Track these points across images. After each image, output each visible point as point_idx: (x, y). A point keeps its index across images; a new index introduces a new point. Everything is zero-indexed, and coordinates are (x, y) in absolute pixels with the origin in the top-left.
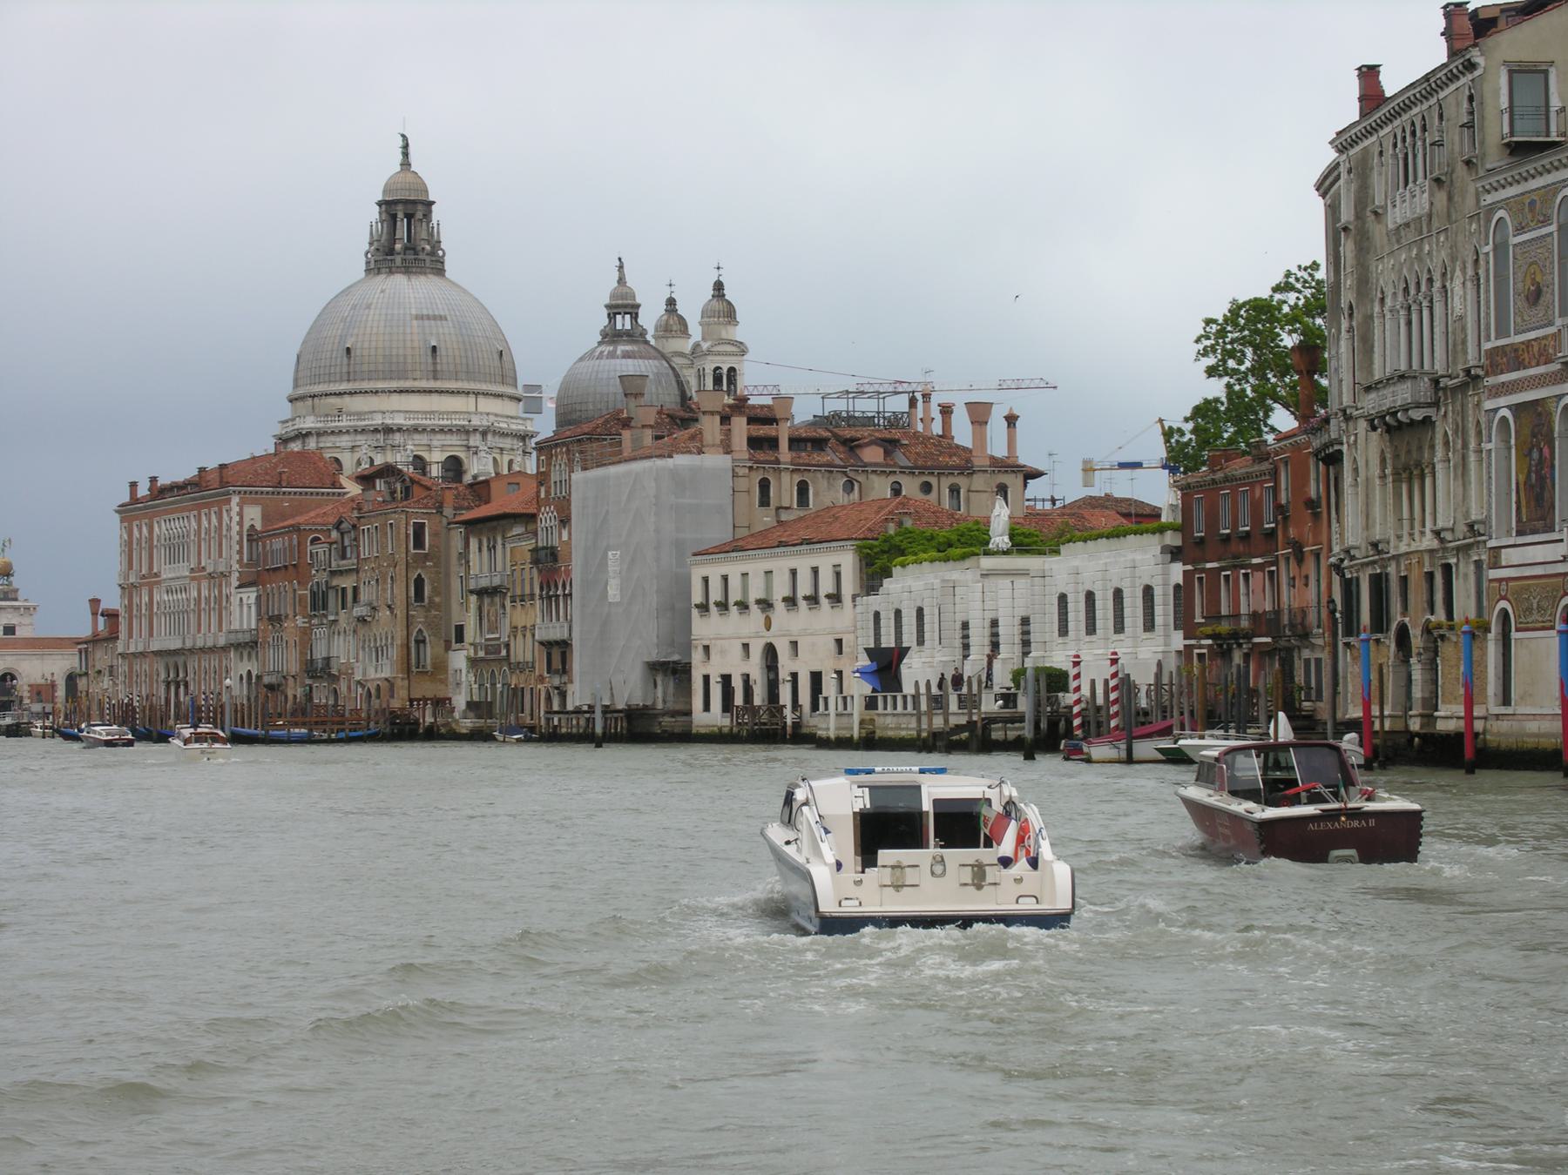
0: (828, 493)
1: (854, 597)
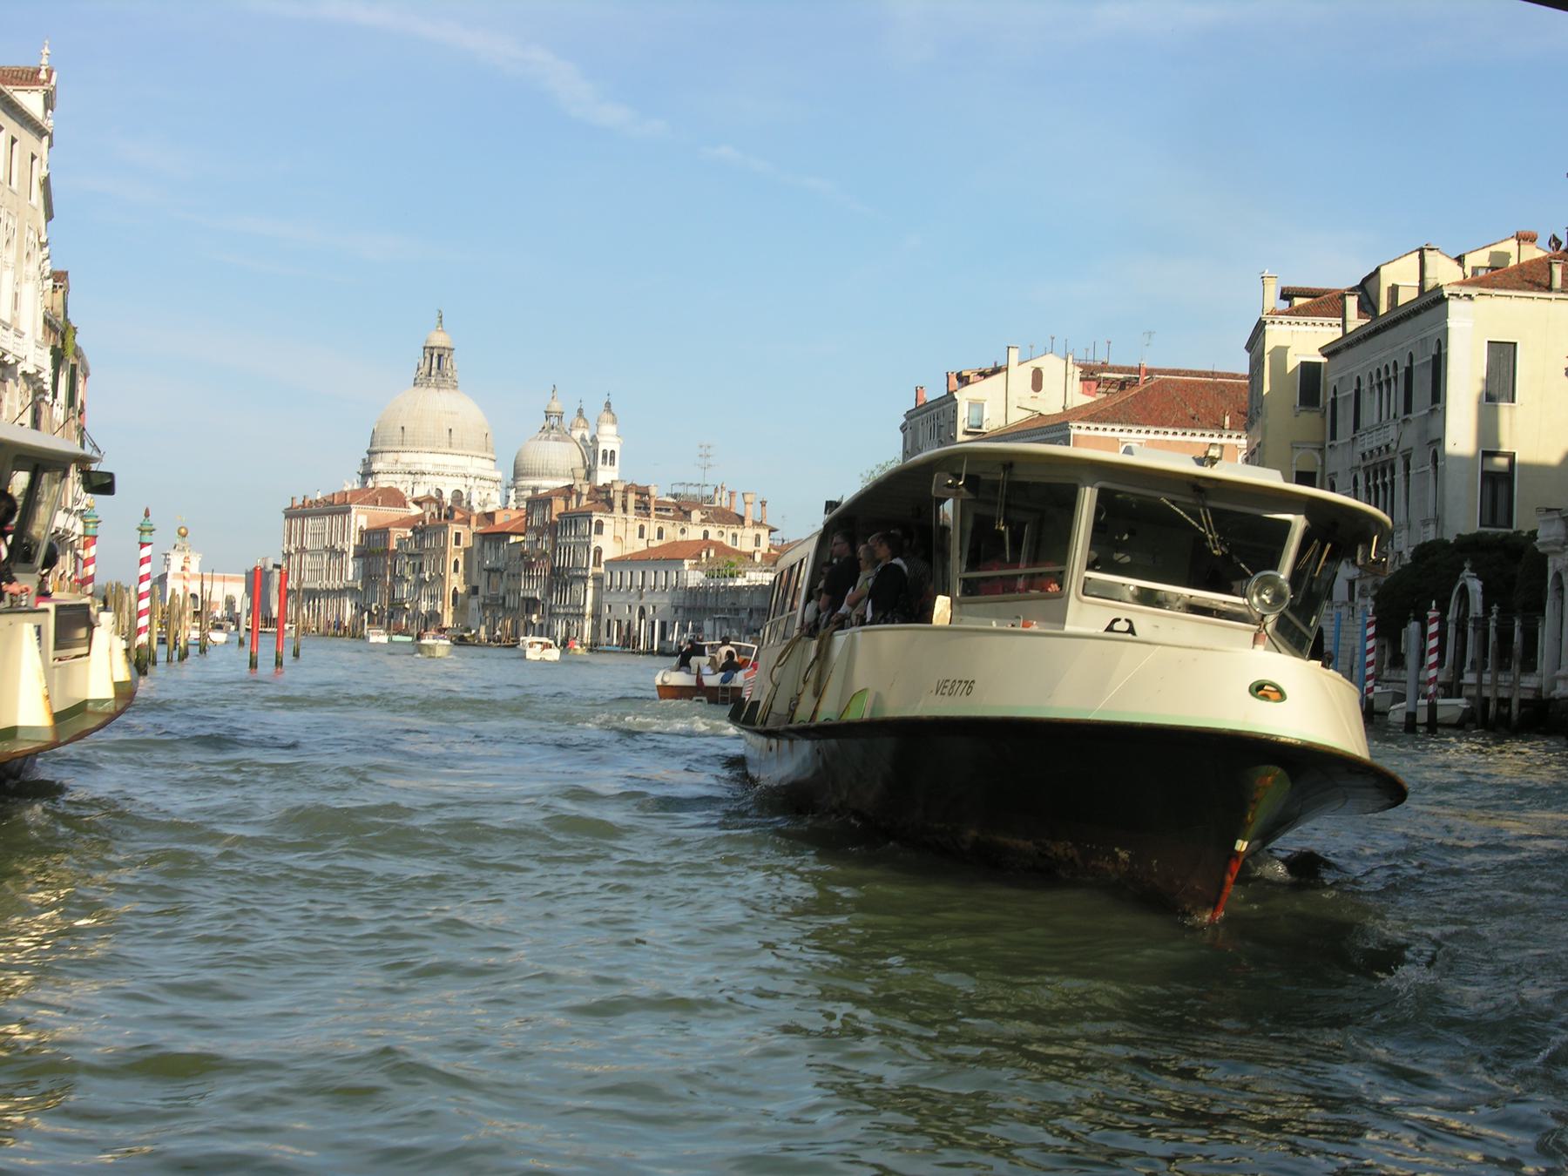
0: (672, 532)
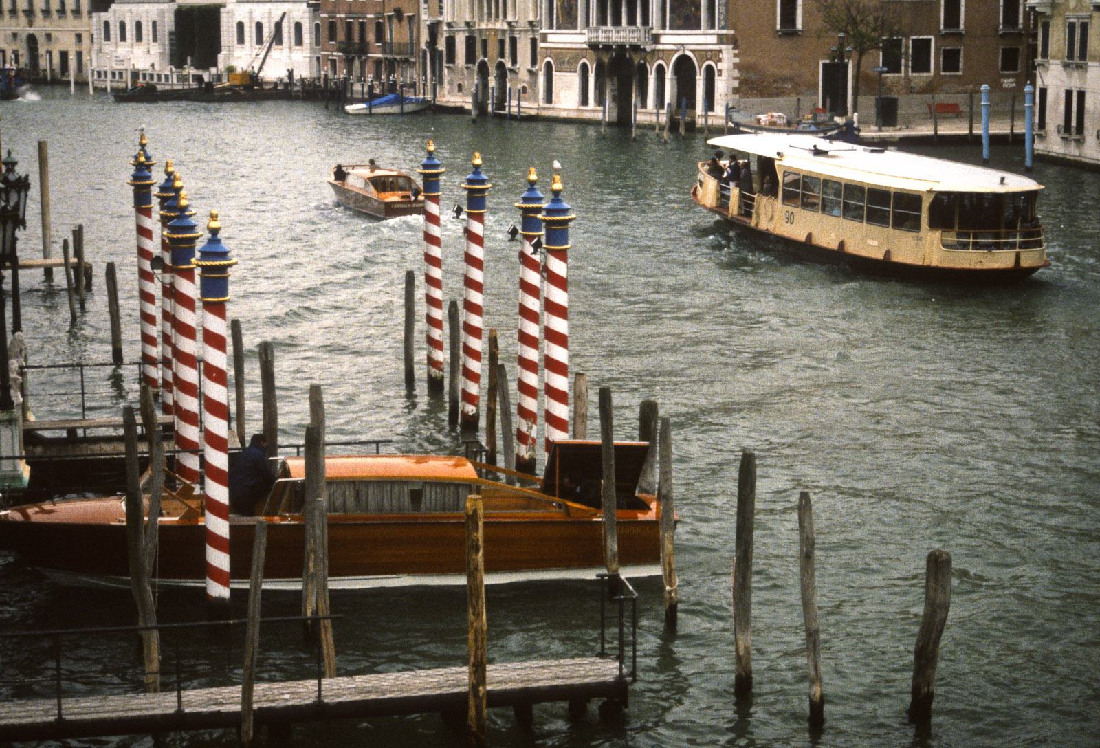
1: (90, 13)
